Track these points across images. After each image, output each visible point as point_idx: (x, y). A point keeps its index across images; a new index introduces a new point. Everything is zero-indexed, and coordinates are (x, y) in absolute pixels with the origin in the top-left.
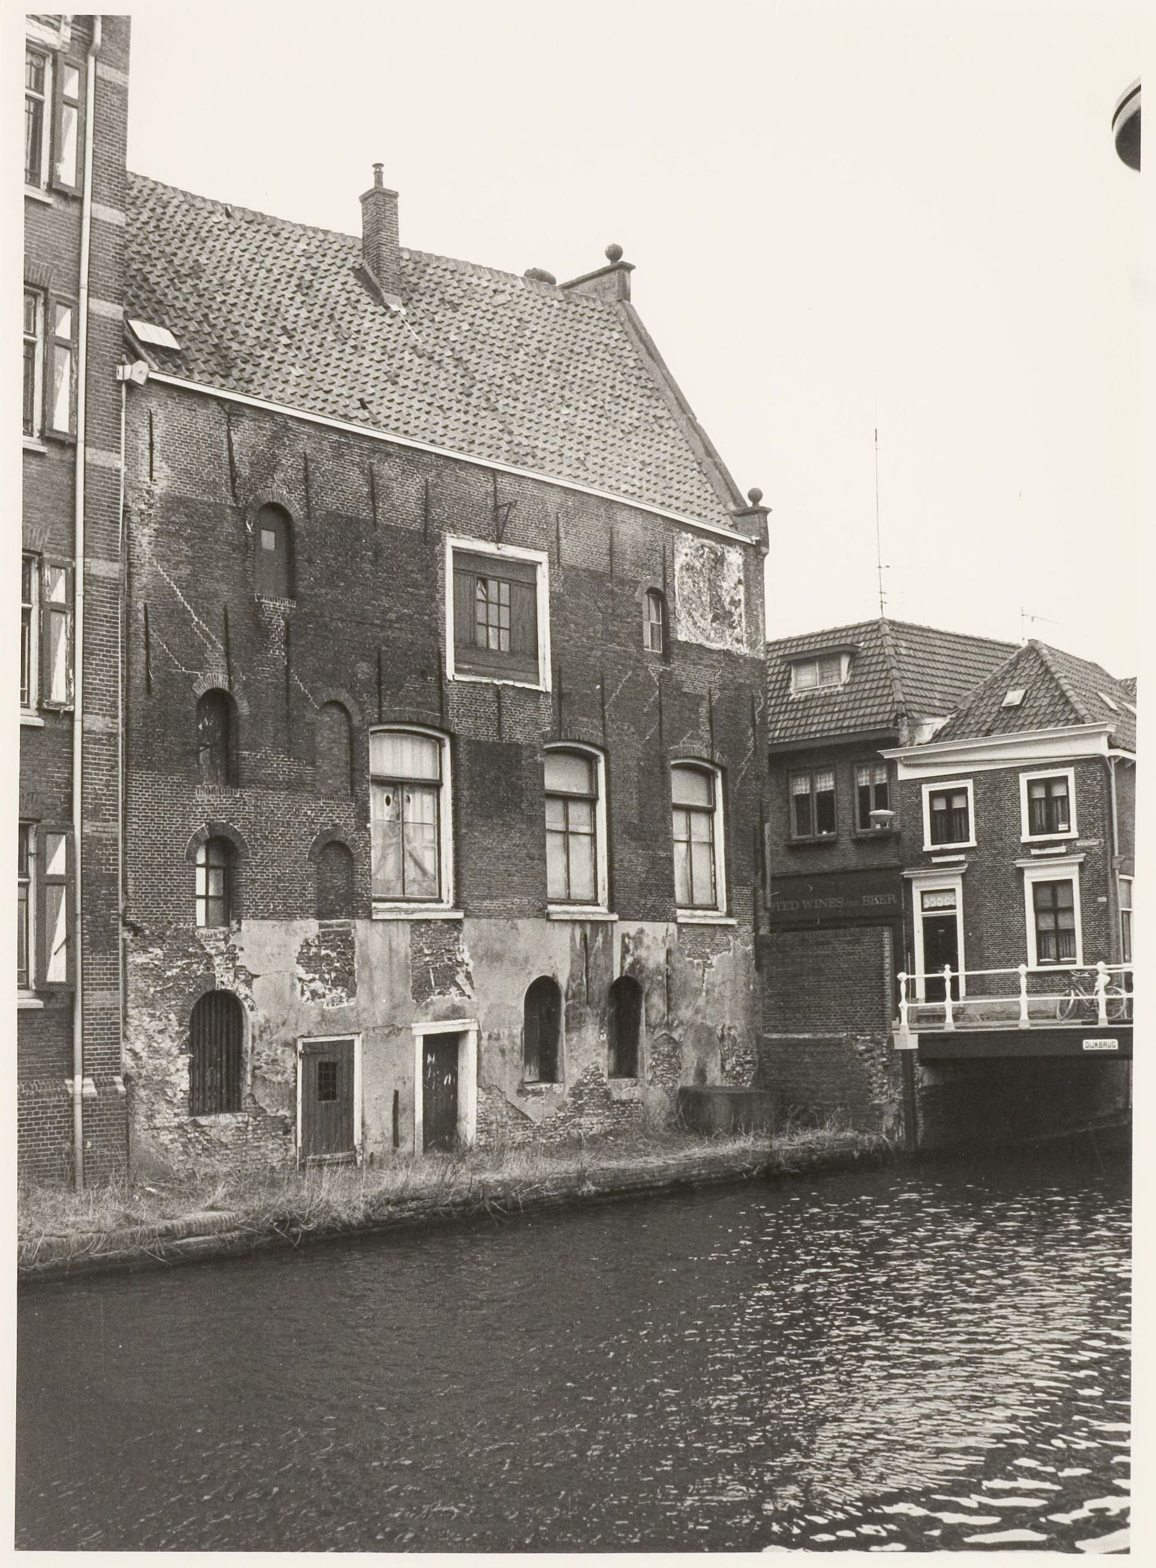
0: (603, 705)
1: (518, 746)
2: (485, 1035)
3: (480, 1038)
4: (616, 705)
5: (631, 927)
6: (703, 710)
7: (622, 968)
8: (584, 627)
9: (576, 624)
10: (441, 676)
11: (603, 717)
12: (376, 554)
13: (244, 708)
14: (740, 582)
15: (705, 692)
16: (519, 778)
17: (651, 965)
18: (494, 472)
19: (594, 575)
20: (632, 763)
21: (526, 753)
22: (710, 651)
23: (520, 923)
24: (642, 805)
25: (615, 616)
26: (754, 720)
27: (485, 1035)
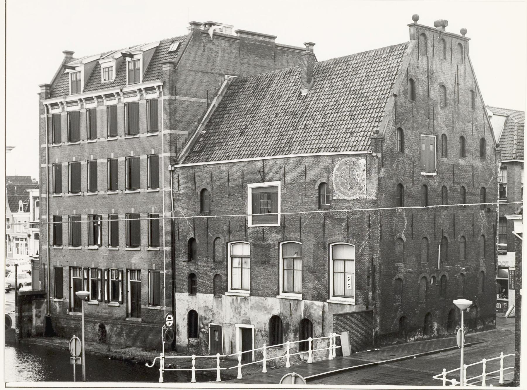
0: (300, 227)
1: (270, 244)
2: (257, 330)
3: (255, 331)
4: (305, 227)
5: (308, 302)
6: (344, 224)
7: (305, 315)
8: (294, 202)
9: (291, 202)
10: (246, 226)
11: (300, 232)
12: (229, 195)
13: (197, 241)
14: (364, 170)
15: (346, 217)
16: (269, 254)
17: (316, 315)
18: (263, 160)
19: (300, 184)
20: (311, 246)
21: (272, 246)
22: (348, 201)
23: (268, 298)
24: (315, 261)
25: (306, 196)
26: (369, 224)
27: (257, 330)
